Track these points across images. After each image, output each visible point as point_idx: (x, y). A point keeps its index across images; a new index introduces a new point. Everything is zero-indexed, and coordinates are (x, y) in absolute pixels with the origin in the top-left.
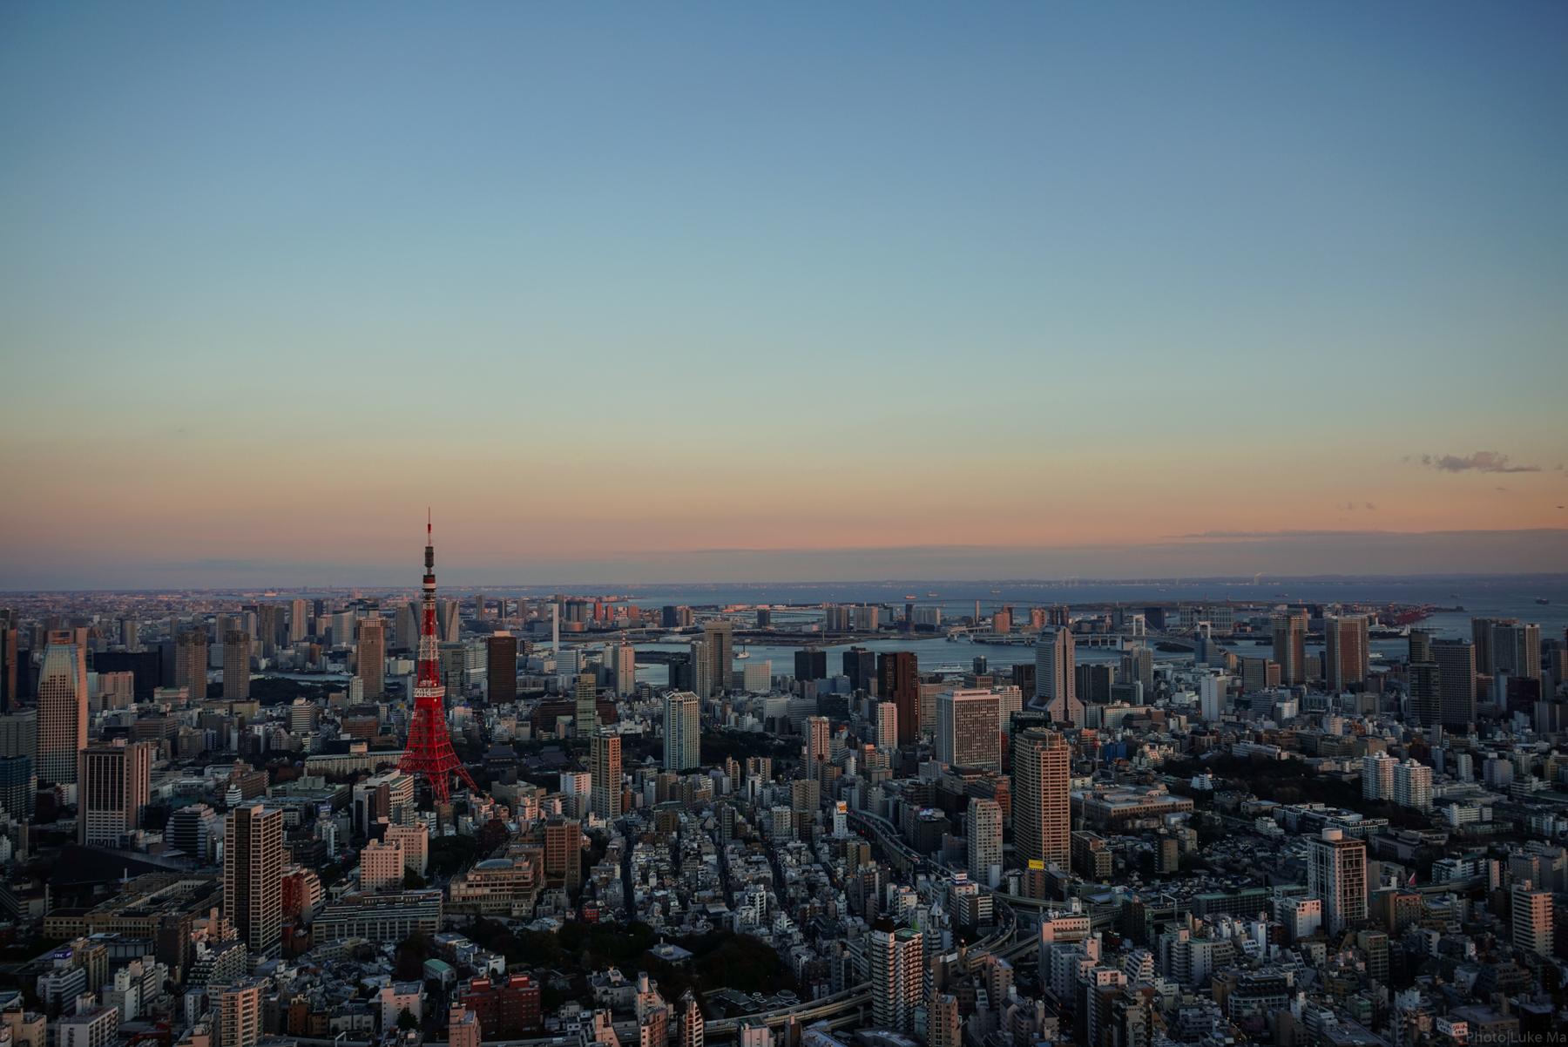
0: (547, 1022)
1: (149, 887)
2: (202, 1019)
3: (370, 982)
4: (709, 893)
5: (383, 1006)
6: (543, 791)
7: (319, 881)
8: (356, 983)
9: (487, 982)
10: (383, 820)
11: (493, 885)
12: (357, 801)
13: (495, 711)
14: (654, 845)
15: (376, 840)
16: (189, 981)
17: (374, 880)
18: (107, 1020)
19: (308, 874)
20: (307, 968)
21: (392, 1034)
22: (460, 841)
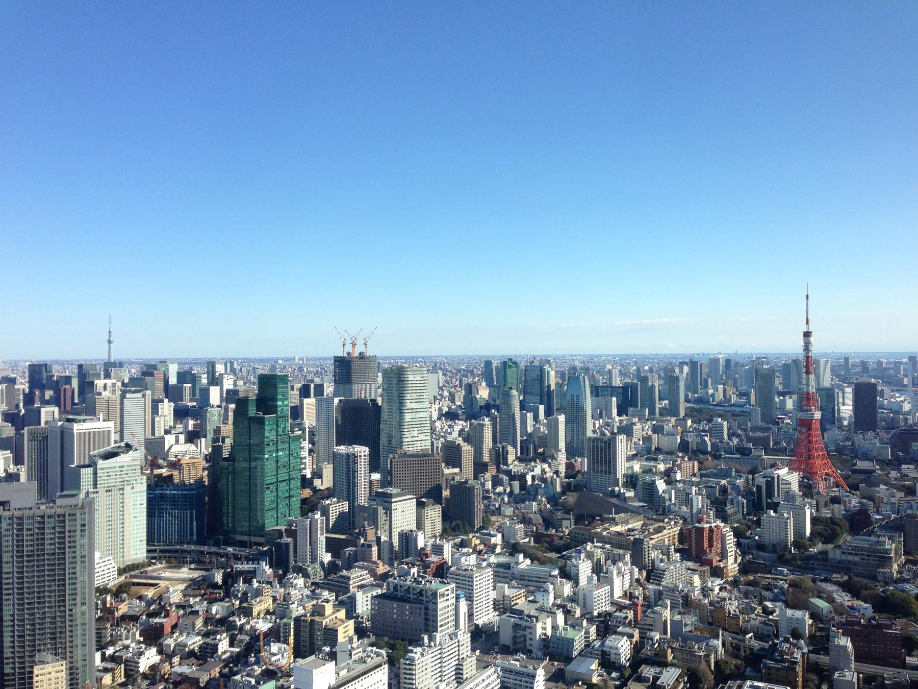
1: (627, 522)
2: (658, 604)
3: (769, 605)
5: (780, 622)
6: (902, 494)
7: (732, 533)
8: (760, 603)
9: (859, 620)
10: (775, 500)
11: (862, 555)
12: (758, 486)
13: (861, 436)
15: (772, 511)
16: (651, 581)
17: (771, 539)
18: (604, 593)
19: (724, 527)
20: (726, 587)
21: (786, 640)
22: (832, 521)
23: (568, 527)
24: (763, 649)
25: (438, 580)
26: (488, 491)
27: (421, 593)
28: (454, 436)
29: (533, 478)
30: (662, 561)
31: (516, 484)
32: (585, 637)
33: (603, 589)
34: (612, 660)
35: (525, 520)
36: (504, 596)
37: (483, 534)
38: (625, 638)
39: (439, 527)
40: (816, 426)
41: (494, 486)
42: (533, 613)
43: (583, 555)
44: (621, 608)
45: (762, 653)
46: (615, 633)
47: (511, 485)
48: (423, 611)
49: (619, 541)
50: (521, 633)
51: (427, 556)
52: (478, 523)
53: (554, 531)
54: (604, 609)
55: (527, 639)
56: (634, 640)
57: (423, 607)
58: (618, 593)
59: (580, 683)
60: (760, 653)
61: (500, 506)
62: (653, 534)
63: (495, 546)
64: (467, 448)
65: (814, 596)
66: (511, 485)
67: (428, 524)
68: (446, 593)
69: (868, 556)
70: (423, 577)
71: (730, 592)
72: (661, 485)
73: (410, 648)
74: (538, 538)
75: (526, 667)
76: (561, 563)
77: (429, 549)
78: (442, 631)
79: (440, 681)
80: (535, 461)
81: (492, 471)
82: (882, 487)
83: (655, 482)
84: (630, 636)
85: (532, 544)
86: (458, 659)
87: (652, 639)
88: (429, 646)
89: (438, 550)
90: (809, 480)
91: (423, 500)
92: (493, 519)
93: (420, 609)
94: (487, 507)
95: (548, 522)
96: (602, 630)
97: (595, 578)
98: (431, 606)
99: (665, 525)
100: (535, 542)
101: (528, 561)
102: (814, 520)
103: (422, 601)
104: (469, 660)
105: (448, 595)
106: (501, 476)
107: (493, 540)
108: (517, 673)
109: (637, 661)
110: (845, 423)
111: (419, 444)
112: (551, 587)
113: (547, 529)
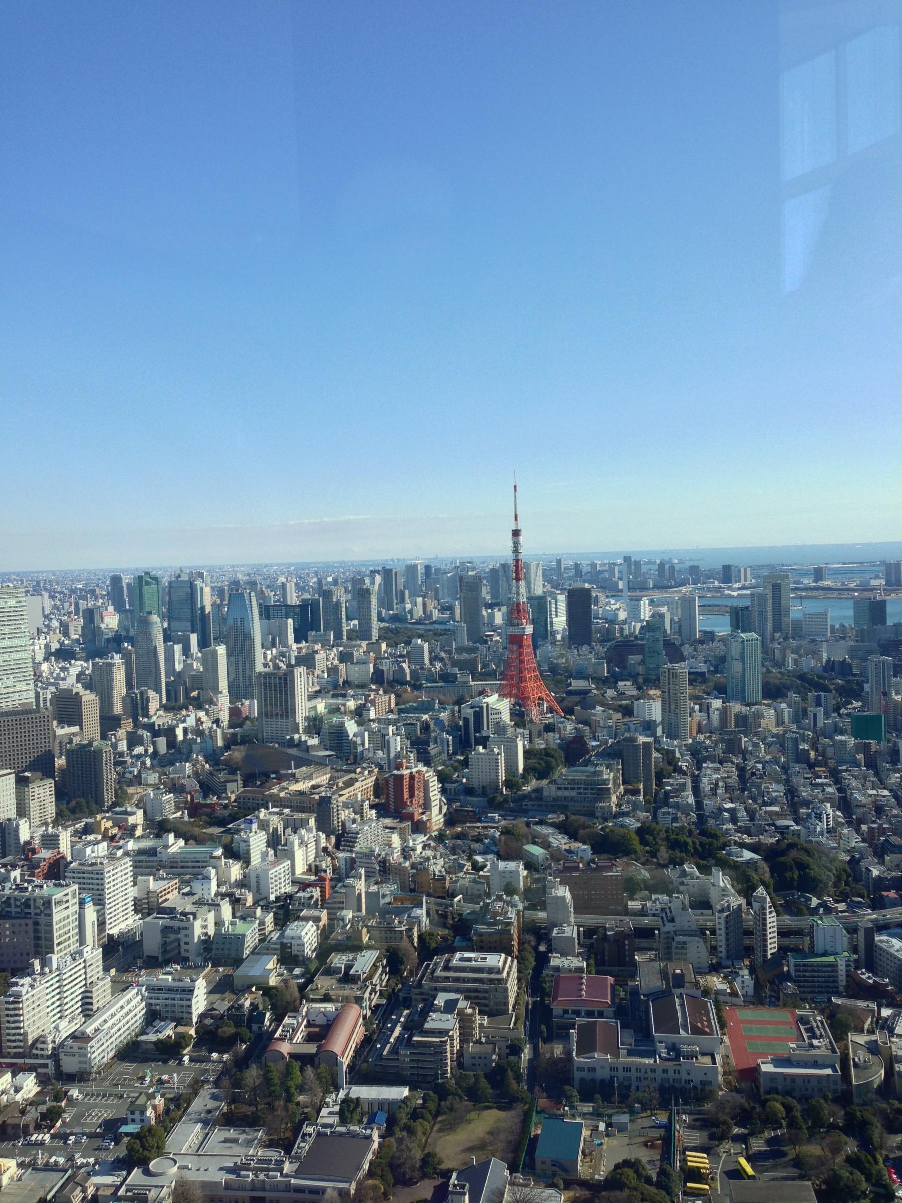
0: (630, 903)
1: (310, 777)
3: (479, 858)
4: (776, 808)
6: (620, 715)
7: (436, 778)
8: (469, 858)
10: (484, 734)
12: (464, 718)
14: (721, 764)
15: (481, 748)
16: (341, 848)
19: (427, 772)
20: (430, 844)
21: (499, 898)
22: (547, 753)
23: (234, 791)
24: (473, 912)
25: (51, 883)
26: (121, 755)
27: (27, 904)
28: (70, 682)
29: (185, 731)
30: (354, 821)
31: (162, 742)
32: (259, 930)
33: (281, 866)
34: (293, 953)
35: (175, 788)
36: (148, 892)
37: (117, 813)
38: (311, 923)
39: (51, 809)
40: (528, 642)
41: (131, 746)
42: (189, 908)
43: (254, 826)
44: (304, 886)
45: (473, 917)
46: (298, 918)
47: (154, 744)
48: (31, 928)
49: (301, 803)
50: (173, 937)
51: (34, 851)
52: (108, 798)
53: (215, 798)
54: (283, 891)
55: (182, 944)
56: (321, 924)
57: (30, 922)
58: (300, 868)
59: (253, 989)
60: (469, 917)
61: (140, 772)
62: (342, 789)
63: (134, 826)
64: (89, 698)
65: (528, 843)
66: (154, 744)
67: (34, 808)
68: (65, 899)
69: (585, 789)
70: (29, 882)
71: (435, 849)
72: (351, 727)
73: (13, 980)
74: (194, 810)
75: (181, 981)
76: (226, 838)
77: (36, 842)
78: (61, 951)
79: (60, 1018)
80: (187, 709)
81: (128, 725)
82: (599, 708)
83: (342, 725)
84: (317, 920)
85: (186, 818)
86: (85, 985)
87: (343, 920)
88: (42, 974)
89: (50, 841)
90: (519, 705)
91: (26, 774)
92: (131, 790)
93: (26, 925)
94: (121, 775)
95: (207, 788)
96: (281, 917)
97: (271, 852)
98: (42, 919)
99: (357, 776)
100: (190, 816)
101: (182, 842)
102: (527, 754)
103: (30, 913)
104: (101, 984)
105: (67, 901)
106: (140, 732)
107: (131, 820)
108: (169, 990)
109: (325, 950)
110: (559, 637)
111: (16, 696)
112: (213, 872)
113: (206, 796)
